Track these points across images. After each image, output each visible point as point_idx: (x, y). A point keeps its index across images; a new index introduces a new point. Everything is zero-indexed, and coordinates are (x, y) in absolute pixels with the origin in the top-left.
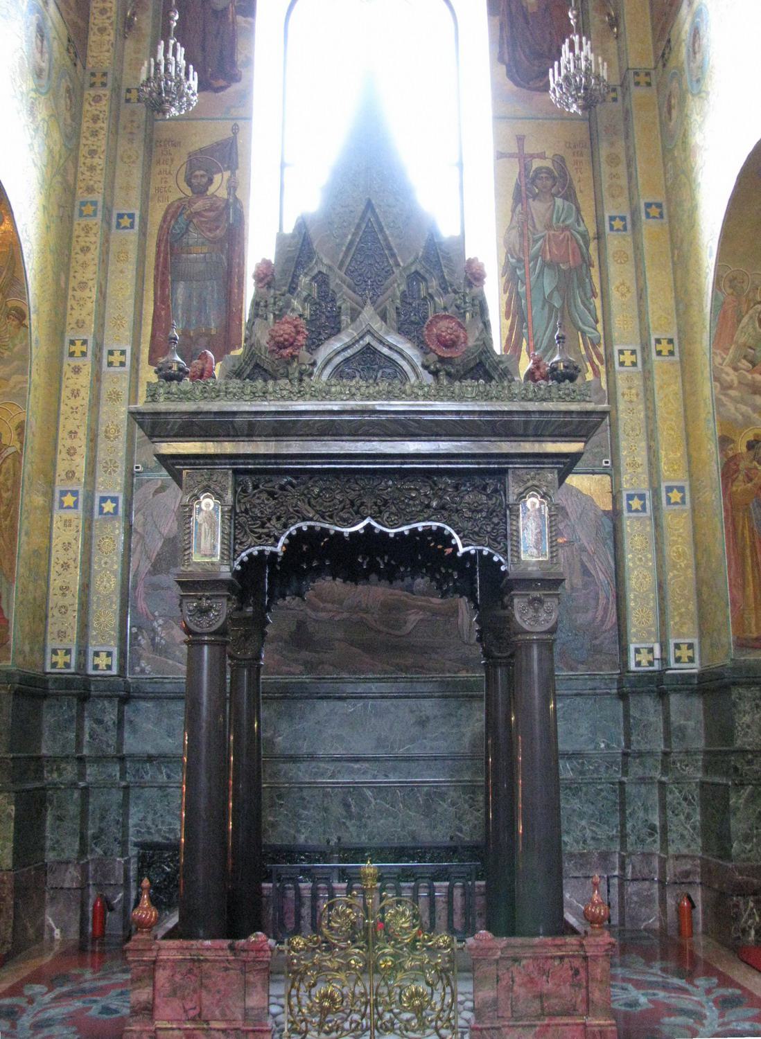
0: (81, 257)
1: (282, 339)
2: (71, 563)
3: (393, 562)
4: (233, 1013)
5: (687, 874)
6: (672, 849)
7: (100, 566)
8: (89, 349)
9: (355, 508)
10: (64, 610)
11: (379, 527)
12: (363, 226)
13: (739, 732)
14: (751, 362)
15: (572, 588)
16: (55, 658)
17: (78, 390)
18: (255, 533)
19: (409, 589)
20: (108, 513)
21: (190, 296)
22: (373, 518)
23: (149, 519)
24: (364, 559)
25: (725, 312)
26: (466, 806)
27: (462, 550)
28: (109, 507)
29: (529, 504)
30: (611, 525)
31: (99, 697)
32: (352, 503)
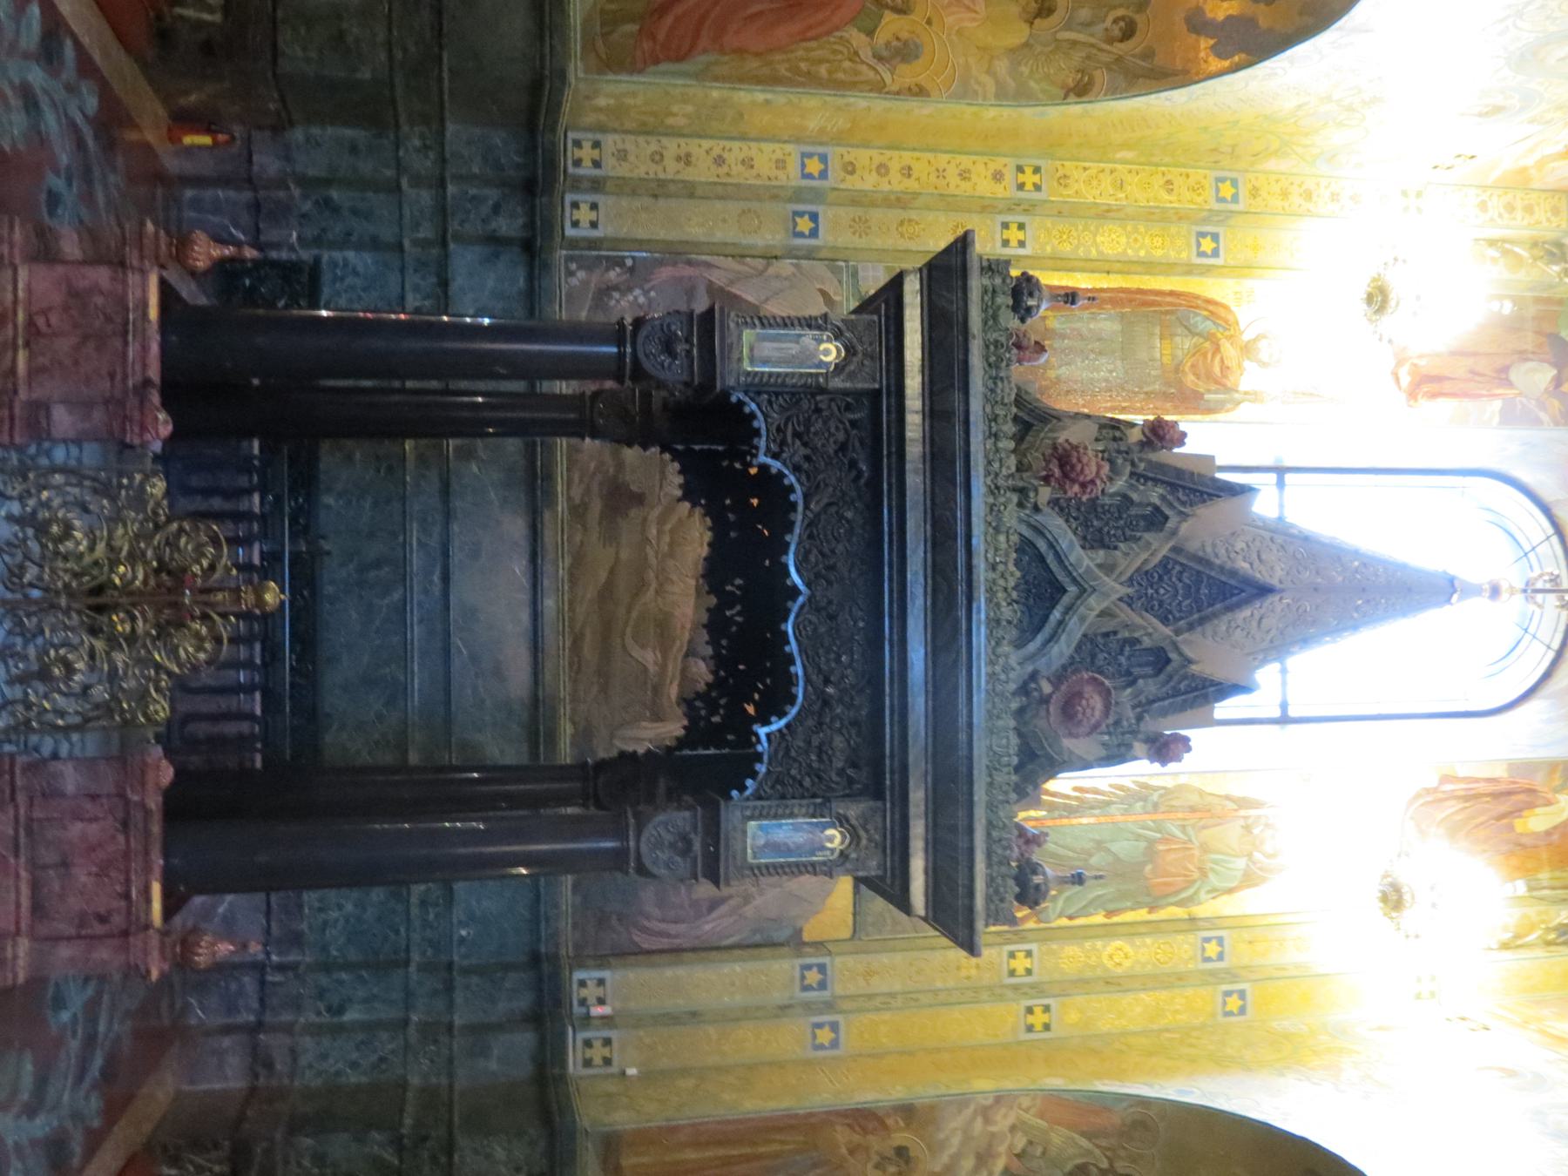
1: (1074, 460)
2: (725, 169)
3: (734, 629)
5: (269, 1065)
6: (308, 1042)
8: (1029, 195)
10: (658, 158)
12: (1233, 582)
14: (1024, 1151)
16: (587, 145)
17: (969, 179)
19: (690, 653)
20: (795, 224)
22: (810, 599)
23: (787, 283)
24: (738, 587)
26: (377, 736)
27: (763, 731)
28: (804, 225)
29: (830, 832)
30: (782, 939)
32: (831, 568)
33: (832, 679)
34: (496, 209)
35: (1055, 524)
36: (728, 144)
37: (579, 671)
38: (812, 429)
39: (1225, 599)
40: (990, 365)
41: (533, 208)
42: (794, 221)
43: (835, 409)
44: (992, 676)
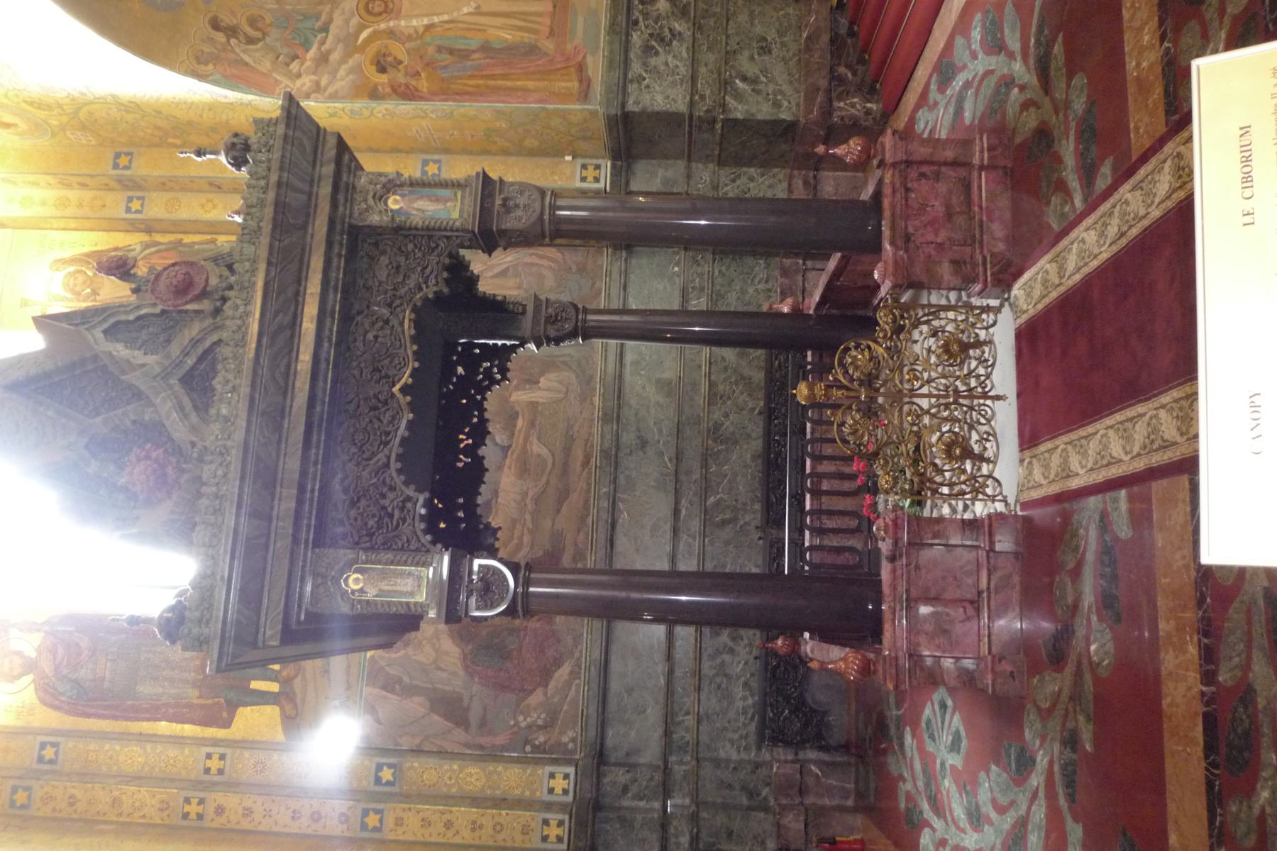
0: (80, 806)
2: (445, 818)
5: (806, 183)
7: (452, 786)
9: (380, 405)
10: (498, 828)
11: (406, 379)
13: (673, 108)
15: (519, 287)
16: (553, 838)
17: (244, 809)
18: (398, 525)
19: (505, 449)
20: (393, 774)
22: (394, 385)
26: (729, 402)
32: (374, 408)
34: (625, 789)
36: (441, 840)
37: (587, 441)
42: (395, 779)
44: (247, 302)
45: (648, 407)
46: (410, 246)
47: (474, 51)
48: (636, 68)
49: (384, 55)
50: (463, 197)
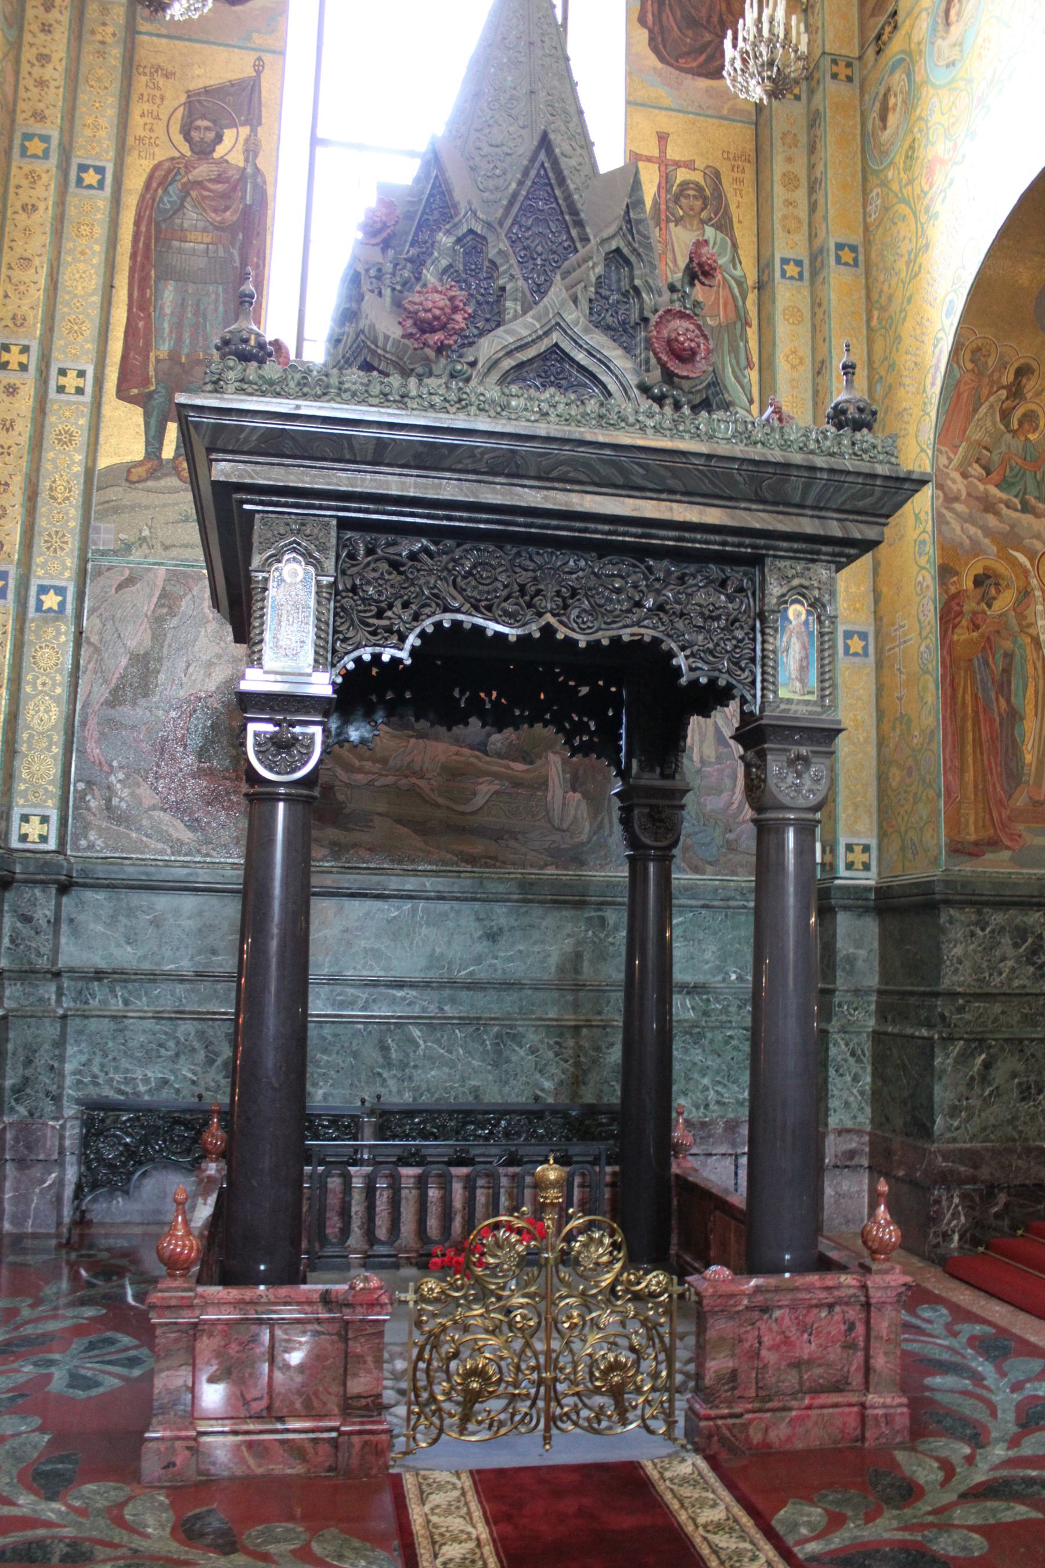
1: (429, 315)
4: (324, 1404)
5: (852, 1154)
7: (35, 687)
8: (33, 360)
9: (527, 598)
12: (533, 173)
13: (947, 969)
14: (984, 468)
15: (702, 762)
17: (12, 421)
18: (368, 625)
19: (482, 747)
20: (50, 610)
21: (183, 304)
22: (554, 615)
23: (109, 625)
24: (462, 693)
25: (959, 395)
26: (551, 1054)
28: (51, 601)
31: (25, 882)
33: (637, 598)
34: (27, 919)
35: (487, 348)
37: (495, 858)
38: (376, 597)
39: (550, 185)
40: (325, 394)
41: (25, 882)
42: (46, 612)
43: (354, 570)
45: (543, 942)
46: (739, 634)
47: (1008, 701)
48: (997, 918)
49: (997, 584)
50: (807, 703)
